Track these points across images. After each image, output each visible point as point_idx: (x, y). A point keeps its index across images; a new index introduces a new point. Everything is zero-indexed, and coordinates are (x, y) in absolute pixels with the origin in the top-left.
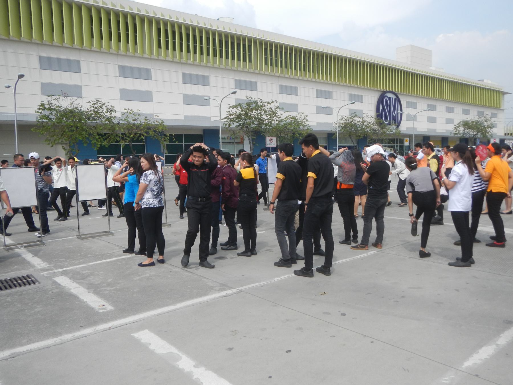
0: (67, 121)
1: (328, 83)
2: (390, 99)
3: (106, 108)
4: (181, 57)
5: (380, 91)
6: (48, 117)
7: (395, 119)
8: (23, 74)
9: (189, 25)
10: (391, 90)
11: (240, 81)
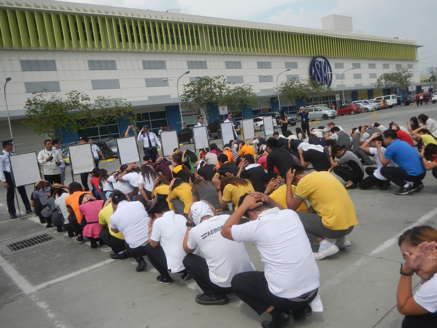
0: (51, 113)
1: (266, 55)
2: (320, 62)
3: (82, 97)
4: (139, 47)
5: (311, 57)
6: (34, 111)
7: (326, 79)
8: (10, 77)
9: (143, 19)
11: (191, 62)
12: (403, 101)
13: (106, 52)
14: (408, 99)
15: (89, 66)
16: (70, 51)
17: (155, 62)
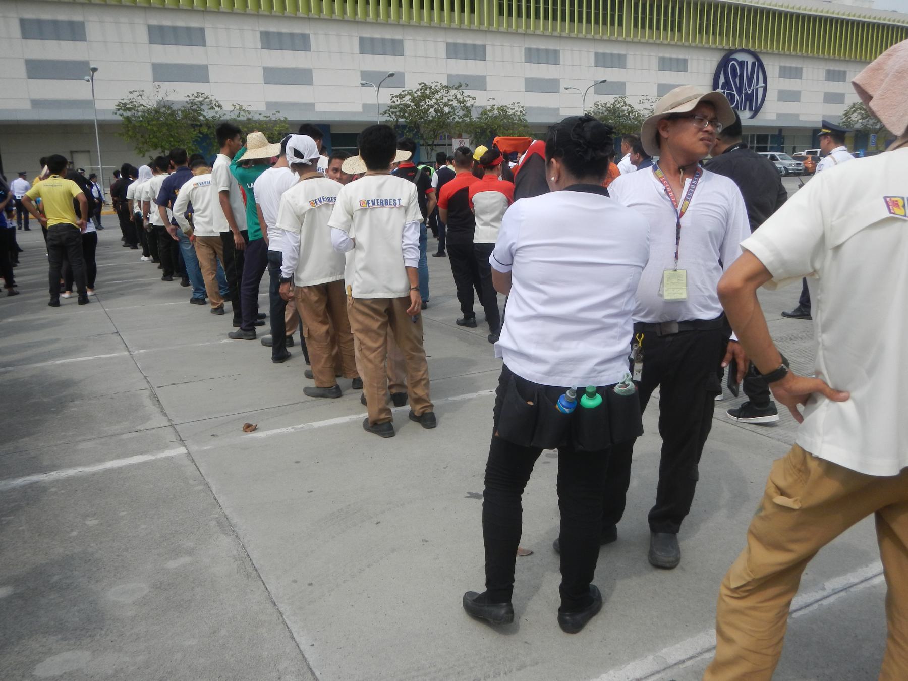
1: (617, 41)
2: (741, 64)
5: (723, 50)
7: (749, 98)
10: (743, 47)
11: (455, 45)
13: (295, 18)
15: (262, 43)
16: (232, 13)
17: (383, 41)
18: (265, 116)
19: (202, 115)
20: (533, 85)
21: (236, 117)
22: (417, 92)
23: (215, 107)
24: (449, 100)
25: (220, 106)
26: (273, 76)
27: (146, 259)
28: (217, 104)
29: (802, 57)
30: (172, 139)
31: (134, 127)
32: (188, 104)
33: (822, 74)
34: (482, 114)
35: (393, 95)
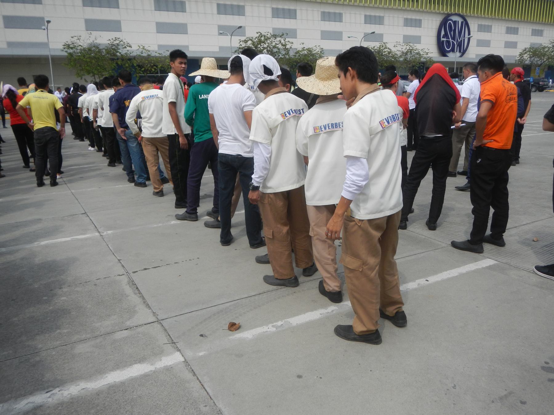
2: (455, 22)
5: (444, 14)
7: (460, 45)
10: (456, 12)
11: (277, 9)
12: (533, 86)
14: (541, 83)
15: (155, 7)
18: (159, 54)
19: (119, 52)
20: (326, 35)
21: (140, 54)
22: (256, 39)
23: (127, 47)
24: (276, 44)
25: (130, 46)
26: (162, 28)
27: (92, 149)
28: (128, 45)
29: (492, 19)
30: (99, 68)
31: (75, 60)
32: (110, 45)
33: (504, 30)
34: (296, 53)
35: (240, 40)
